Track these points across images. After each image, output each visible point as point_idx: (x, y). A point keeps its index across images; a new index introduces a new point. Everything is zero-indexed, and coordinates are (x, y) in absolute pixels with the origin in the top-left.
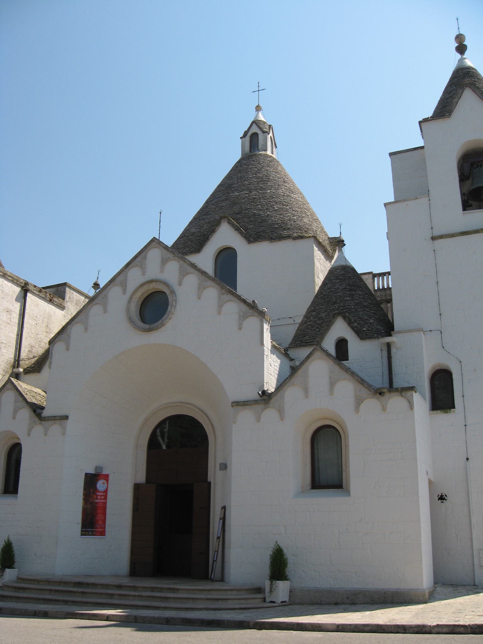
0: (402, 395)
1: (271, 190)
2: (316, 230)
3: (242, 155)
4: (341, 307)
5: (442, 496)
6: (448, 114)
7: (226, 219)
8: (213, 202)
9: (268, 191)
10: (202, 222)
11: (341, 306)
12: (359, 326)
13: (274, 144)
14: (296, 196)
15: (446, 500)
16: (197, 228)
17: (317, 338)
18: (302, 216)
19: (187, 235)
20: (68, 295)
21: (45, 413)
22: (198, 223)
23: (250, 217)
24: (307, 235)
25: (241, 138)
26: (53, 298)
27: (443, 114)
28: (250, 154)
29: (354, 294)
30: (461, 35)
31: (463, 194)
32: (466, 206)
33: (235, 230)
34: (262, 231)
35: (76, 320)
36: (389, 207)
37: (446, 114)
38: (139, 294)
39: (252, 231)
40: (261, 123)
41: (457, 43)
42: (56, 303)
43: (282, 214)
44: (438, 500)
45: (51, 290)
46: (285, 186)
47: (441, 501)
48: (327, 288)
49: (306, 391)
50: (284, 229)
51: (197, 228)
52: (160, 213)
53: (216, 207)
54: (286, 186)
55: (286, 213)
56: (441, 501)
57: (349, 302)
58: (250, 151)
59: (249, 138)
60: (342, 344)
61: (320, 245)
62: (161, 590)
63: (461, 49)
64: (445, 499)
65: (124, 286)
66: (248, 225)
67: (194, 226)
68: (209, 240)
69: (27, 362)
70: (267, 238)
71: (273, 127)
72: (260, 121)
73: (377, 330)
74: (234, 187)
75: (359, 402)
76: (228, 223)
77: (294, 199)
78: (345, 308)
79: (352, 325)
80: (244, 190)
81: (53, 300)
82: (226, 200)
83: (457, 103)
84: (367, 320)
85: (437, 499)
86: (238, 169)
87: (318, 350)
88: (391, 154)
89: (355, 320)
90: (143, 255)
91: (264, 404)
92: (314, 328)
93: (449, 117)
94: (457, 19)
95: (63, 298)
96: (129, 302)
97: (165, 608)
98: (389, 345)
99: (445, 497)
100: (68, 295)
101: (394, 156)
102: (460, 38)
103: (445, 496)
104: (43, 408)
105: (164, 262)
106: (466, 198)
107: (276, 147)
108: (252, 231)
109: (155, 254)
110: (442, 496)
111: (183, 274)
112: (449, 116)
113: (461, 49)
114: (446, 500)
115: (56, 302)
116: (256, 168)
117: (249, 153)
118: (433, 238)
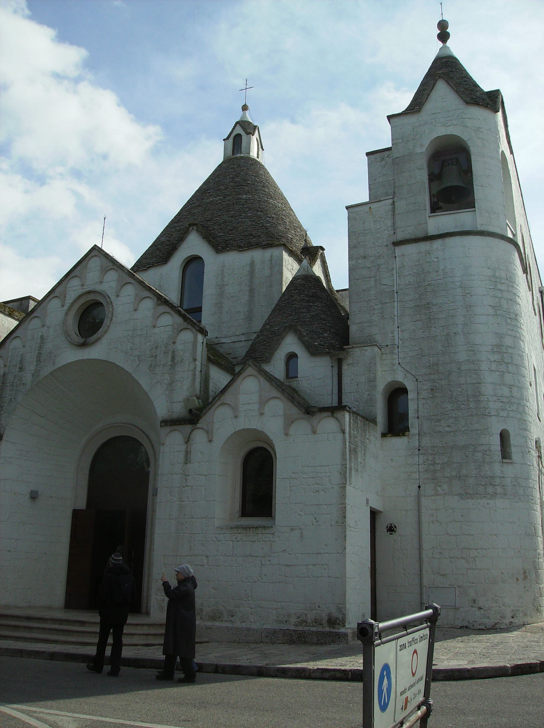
0: (333, 416)
1: (247, 195)
2: (292, 238)
3: (224, 159)
4: (296, 320)
5: (391, 527)
6: (418, 107)
7: (195, 228)
8: (187, 208)
9: (244, 196)
10: (173, 230)
11: (295, 318)
12: (310, 340)
13: (261, 146)
14: (275, 202)
15: (395, 531)
16: (167, 237)
17: (266, 354)
18: (278, 223)
19: (157, 244)
22: (168, 231)
23: (220, 225)
25: (224, 140)
26: (13, 312)
27: (412, 108)
28: (232, 157)
29: (311, 305)
30: (444, 20)
31: (431, 196)
32: (435, 208)
33: (204, 238)
34: (231, 239)
35: (15, 335)
36: (351, 210)
37: (416, 108)
39: (221, 239)
41: (439, 30)
42: (16, 318)
44: (387, 532)
45: (15, 304)
46: (263, 191)
47: (390, 533)
48: (284, 299)
49: (235, 409)
51: (167, 237)
52: (105, 218)
53: (189, 214)
54: (265, 191)
55: (259, 220)
56: (390, 533)
57: (304, 314)
58: (233, 154)
59: (232, 140)
61: (291, 253)
62: (82, 623)
63: (443, 36)
64: (395, 530)
65: (63, 297)
66: (218, 233)
67: (165, 234)
68: (177, 249)
70: (235, 246)
71: (259, 128)
72: (245, 121)
73: (330, 345)
74: (208, 193)
75: (289, 422)
77: (272, 204)
78: (299, 320)
79: (303, 339)
80: (218, 195)
81: (13, 314)
82: (199, 206)
83: (429, 95)
84: (320, 334)
85: (386, 531)
86: (218, 173)
87: (250, 365)
88: (368, 154)
89: (307, 334)
90: (83, 264)
92: (265, 343)
93: (419, 111)
94: (441, 4)
96: (66, 314)
97: (56, 642)
99: (395, 528)
101: (371, 156)
102: (443, 26)
103: (394, 528)
105: (104, 271)
106: (435, 200)
107: (263, 150)
108: (221, 239)
109: (95, 263)
110: (391, 527)
112: (419, 110)
113: (443, 36)
114: (395, 531)
115: (17, 316)
116: (235, 171)
117: (230, 157)
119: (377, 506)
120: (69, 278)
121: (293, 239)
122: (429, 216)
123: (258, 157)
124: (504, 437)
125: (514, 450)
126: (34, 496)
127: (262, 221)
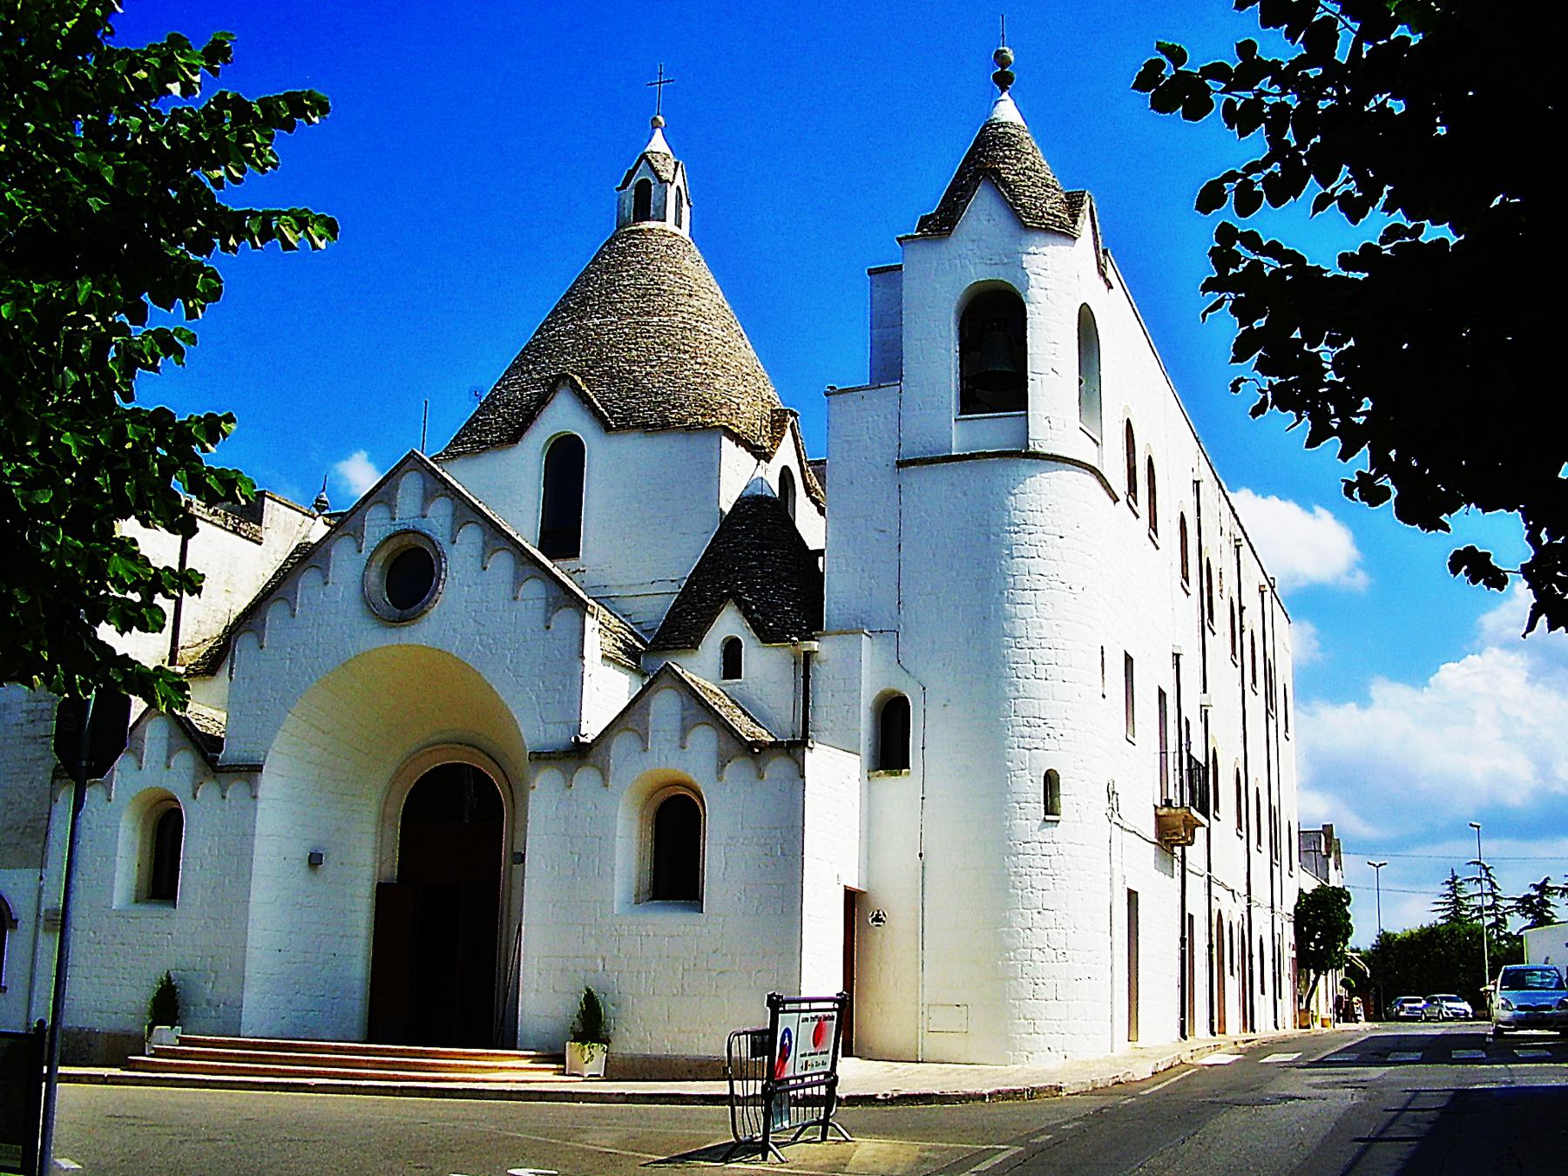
2: (738, 404)
9: (656, 319)
14: (711, 327)
20: (270, 516)
21: (224, 756)
24: (714, 419)
26: (239, 524)
38: (384, 554)
40: (659, 158)
43: (673, 372)
50: (674, 407)
54: (693, 307)
57: (754, 571)
60: (732, 650)
65: (358, 536)
69: (191, 652)
76: (571, 387)
77: (705, 334)
91: (580, 758)
95: (260, 524)
96: (368, 566)
98: (808, 656)
100: (270, 516)
104: (215, 743)
105: (428, 497)
111: (458, 523)
116: (638, 262)
118: (900, 464)
119: (854, 885)
120: (367, 505)
121: (741, 406)
122: (956, 420)
123: (680, 227)
124: (1051, 781)
125: (1065, 802)
126: (315, 860)
127: (686, 373)
